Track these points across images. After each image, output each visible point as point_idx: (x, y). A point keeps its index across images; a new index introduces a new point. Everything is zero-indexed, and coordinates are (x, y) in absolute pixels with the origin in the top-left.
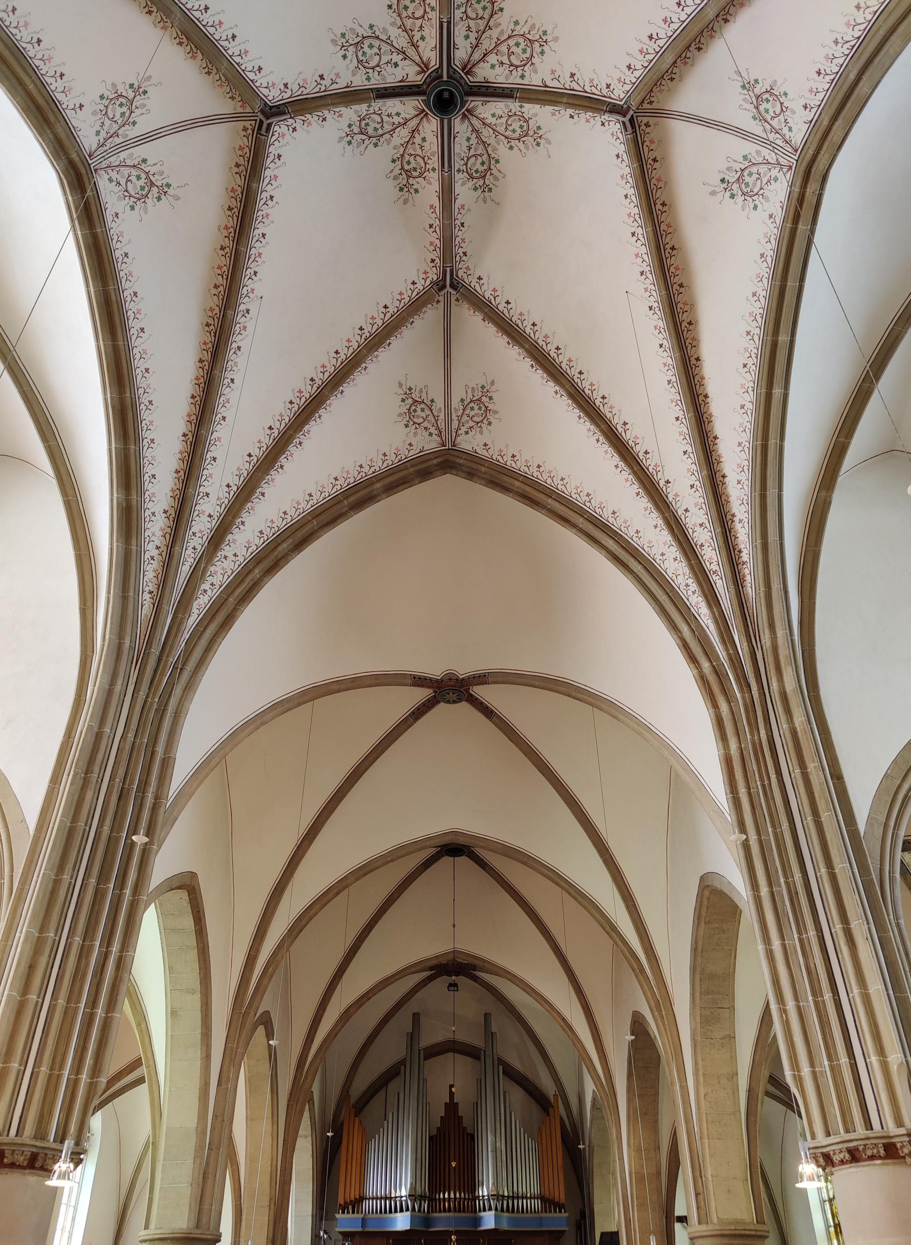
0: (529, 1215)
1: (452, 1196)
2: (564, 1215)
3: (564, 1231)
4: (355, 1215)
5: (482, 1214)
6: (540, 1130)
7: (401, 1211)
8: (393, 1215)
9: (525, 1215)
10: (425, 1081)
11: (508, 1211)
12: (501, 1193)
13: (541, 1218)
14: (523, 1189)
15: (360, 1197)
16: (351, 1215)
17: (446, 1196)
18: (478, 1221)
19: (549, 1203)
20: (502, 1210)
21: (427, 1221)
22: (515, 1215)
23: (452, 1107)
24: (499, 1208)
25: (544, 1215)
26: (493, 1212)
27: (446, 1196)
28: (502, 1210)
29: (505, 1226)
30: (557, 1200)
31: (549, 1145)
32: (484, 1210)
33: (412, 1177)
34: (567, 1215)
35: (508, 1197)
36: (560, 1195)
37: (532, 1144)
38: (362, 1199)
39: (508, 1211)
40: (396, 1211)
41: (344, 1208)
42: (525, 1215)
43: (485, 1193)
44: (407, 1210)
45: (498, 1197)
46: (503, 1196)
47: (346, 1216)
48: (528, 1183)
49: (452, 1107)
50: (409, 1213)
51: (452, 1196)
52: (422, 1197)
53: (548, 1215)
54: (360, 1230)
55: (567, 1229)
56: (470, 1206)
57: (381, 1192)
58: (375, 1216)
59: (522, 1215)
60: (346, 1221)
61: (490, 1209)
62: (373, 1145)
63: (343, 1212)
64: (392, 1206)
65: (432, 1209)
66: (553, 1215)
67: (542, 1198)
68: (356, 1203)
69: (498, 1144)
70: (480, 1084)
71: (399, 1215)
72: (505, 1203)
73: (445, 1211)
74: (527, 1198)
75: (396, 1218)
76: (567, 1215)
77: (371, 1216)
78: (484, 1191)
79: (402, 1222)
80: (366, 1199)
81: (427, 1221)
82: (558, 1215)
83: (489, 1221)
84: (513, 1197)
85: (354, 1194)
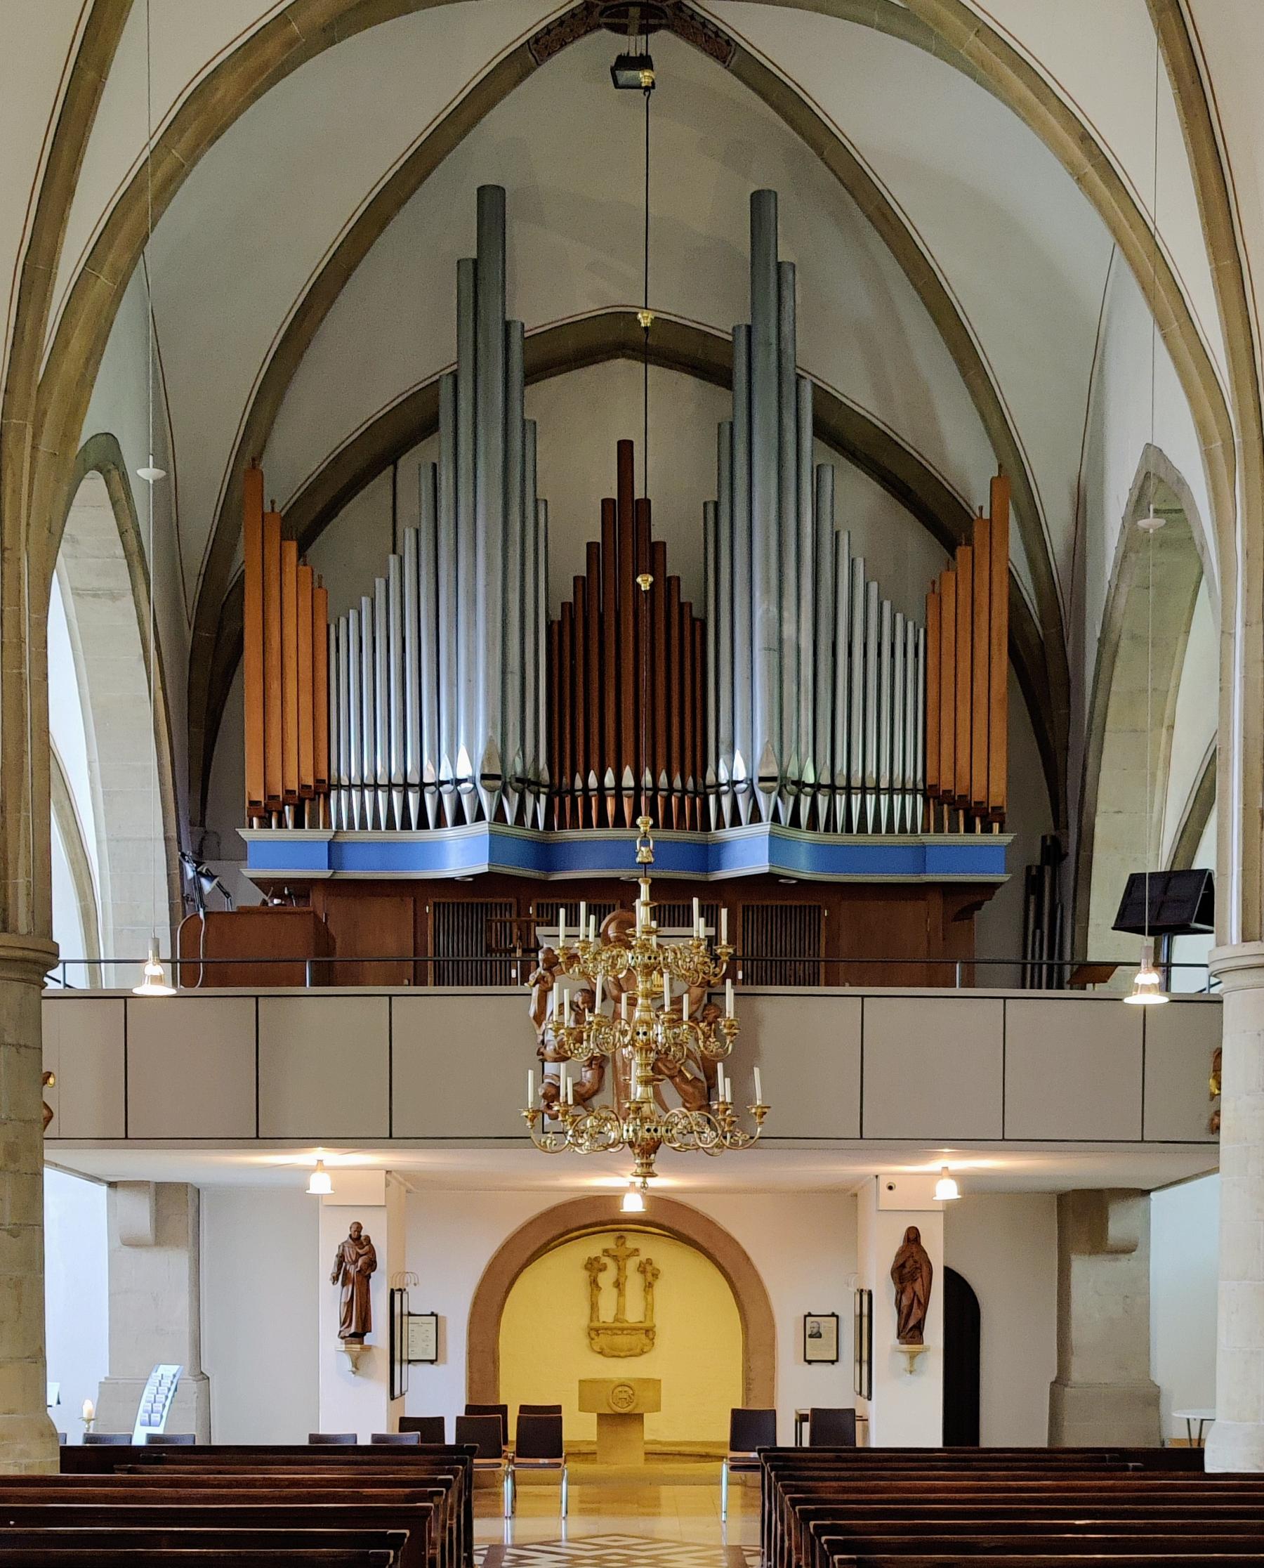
0: (884, 839)
1: (628, 780)
2: (998, 838)
3: (994, 886)
4: (306, 834)
5: (728, 833)
6: (934, 594)
7: (459, 819)
8: (432, 834)
9: (869, 839)
10: (529, 427)
11: (813, 824)
12: (792, 773)
13: (923, 847)
14: (864, 764)
15: (318, 781)
16: (290, 833)
17: (609, 780)
18: (710, 854)
19: (950, 805)
20: (795, 822)
21: (546, 853)
22: (840, 838)
23: (627, 515)
24: (785, 815)
25: (932, 839)
26: (765, 827)
27: (609, 780)
28: (795, 822)
29: (802, 868)
30: (978, 795)
31: (965, 636)
32: (736, 821)
33: (490, 723)
34: (1007, 838)
35: (817, 787)
36: (992, 785)
37: (906, 632)
38: (323, 788)
39: (813, 824)
40: (440, 823)
41: (267, 813)
42: (869, 839)
43: (740, 773)
44: (480, 816)
45: (785, 784)
46: (800, 784)
47: (273, 833)
48: (888, 751)
49: (627, 515)
50: (483, 827)
51: (628, 780)
52: (526, 784)
53: (947, 838)
54: (326, 874)
55: (1004, 878)
56: (691, 807)
57: (385, 766)
58: (370, 835)
59: (855, 839)
60: (276, 851)
61: (756, 817)
62: (351, 629)
63: (265, 824)
64: (428, 808)
65: (559, 815)
66: (962, 838)
67: (931, 794)
68: (306, 802)
69: (789, 630)
70: (730, 443)
71: (450, 832)
72: (805, 803)
73: (603, 823)
74: (877, 790)
75: (440, 844)
76: (1007, 838)
77: (357, 835)
78: (735, 768)
79: (461, 853)
80: (339, 787)
81: (546, 853)
82: (978, 838)
83: (748, 851)
84: (833, 788)
85: (296, 772)
